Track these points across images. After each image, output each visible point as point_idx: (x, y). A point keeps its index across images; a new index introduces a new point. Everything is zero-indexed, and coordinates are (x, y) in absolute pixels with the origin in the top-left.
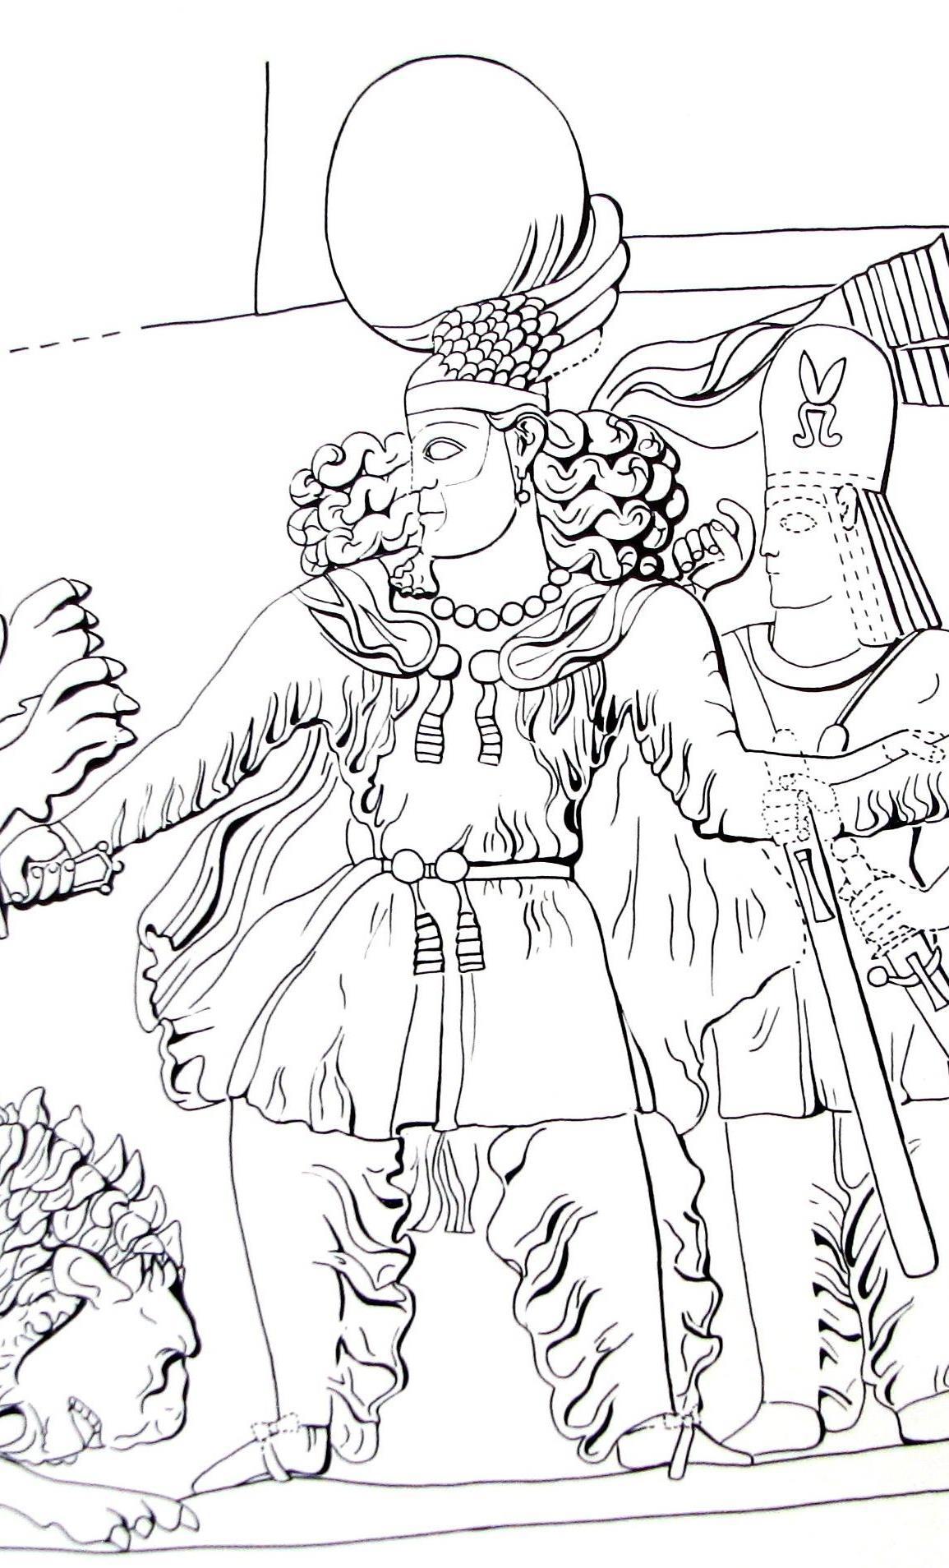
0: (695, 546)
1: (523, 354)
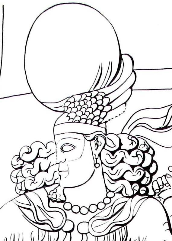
0: (160, 183)
1: (97, 113)
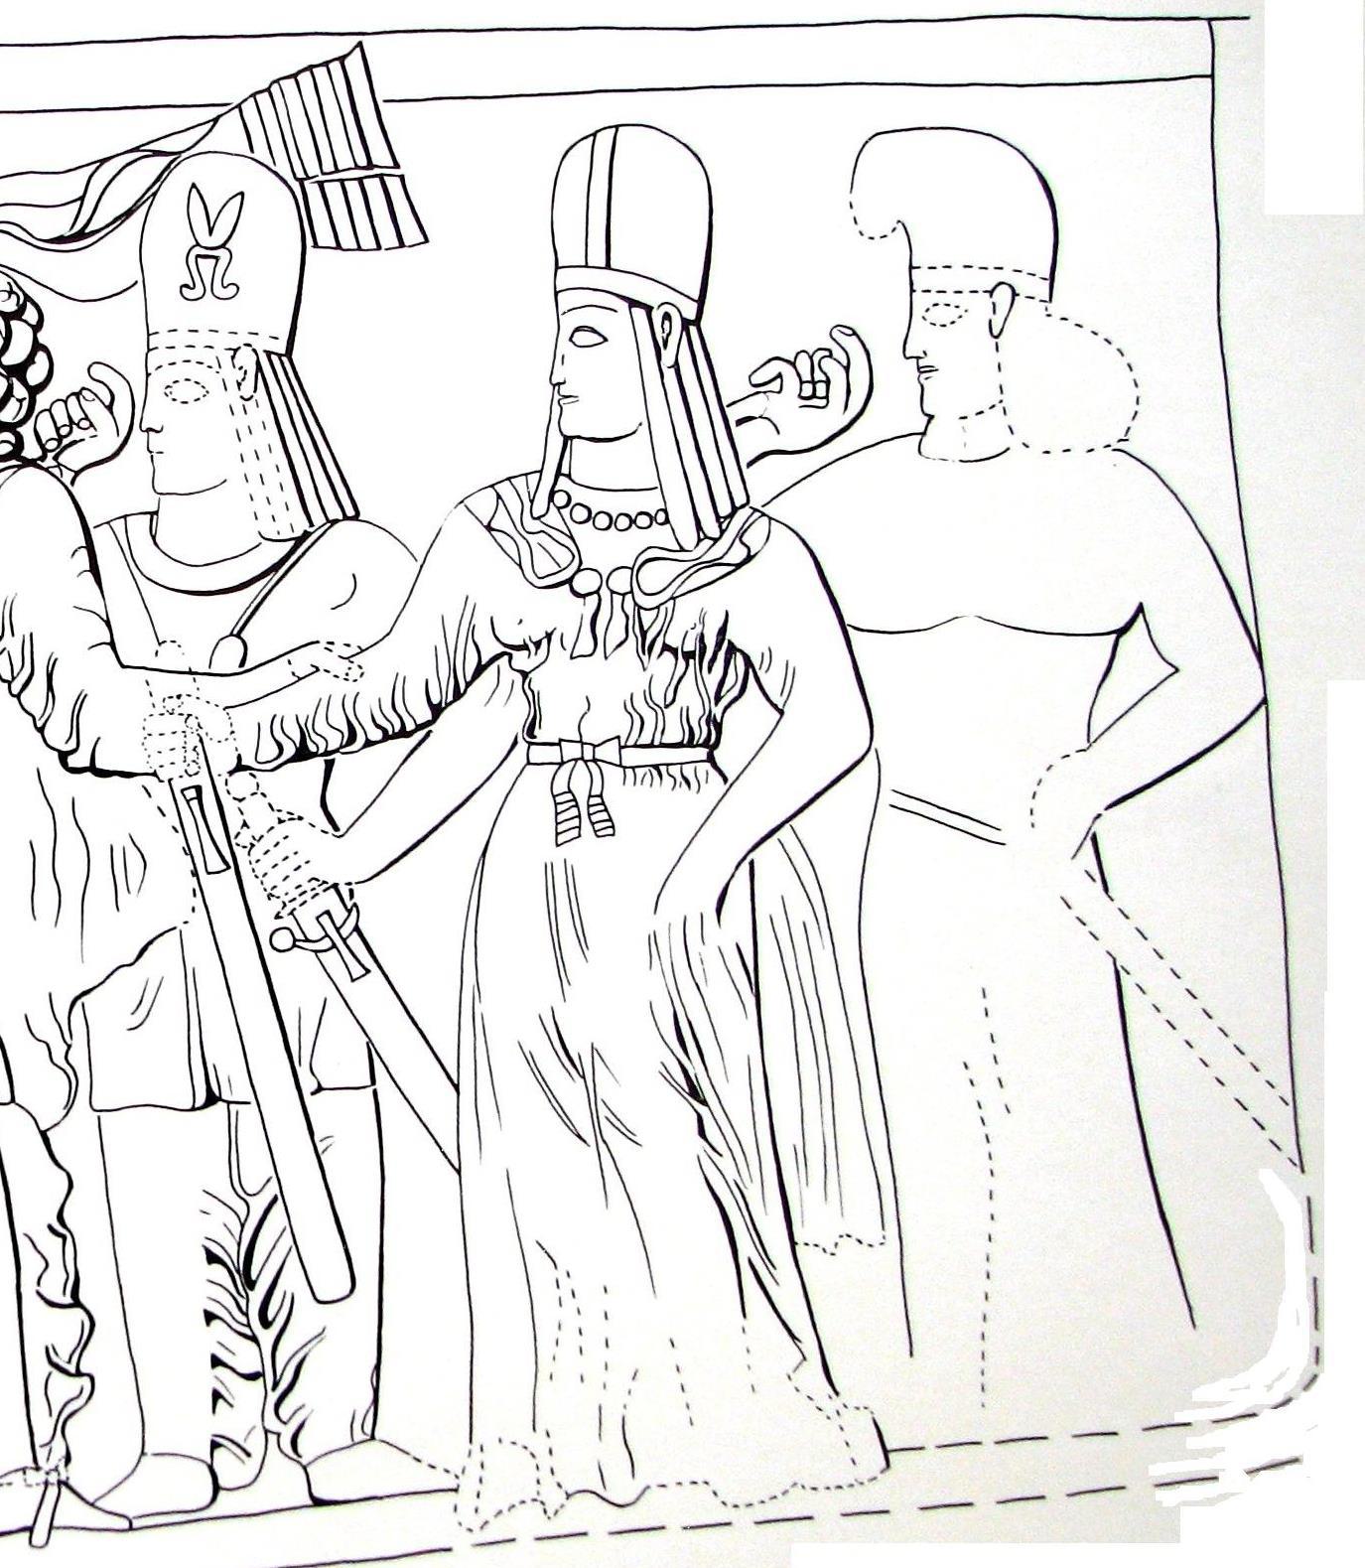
0: (62, 419)
